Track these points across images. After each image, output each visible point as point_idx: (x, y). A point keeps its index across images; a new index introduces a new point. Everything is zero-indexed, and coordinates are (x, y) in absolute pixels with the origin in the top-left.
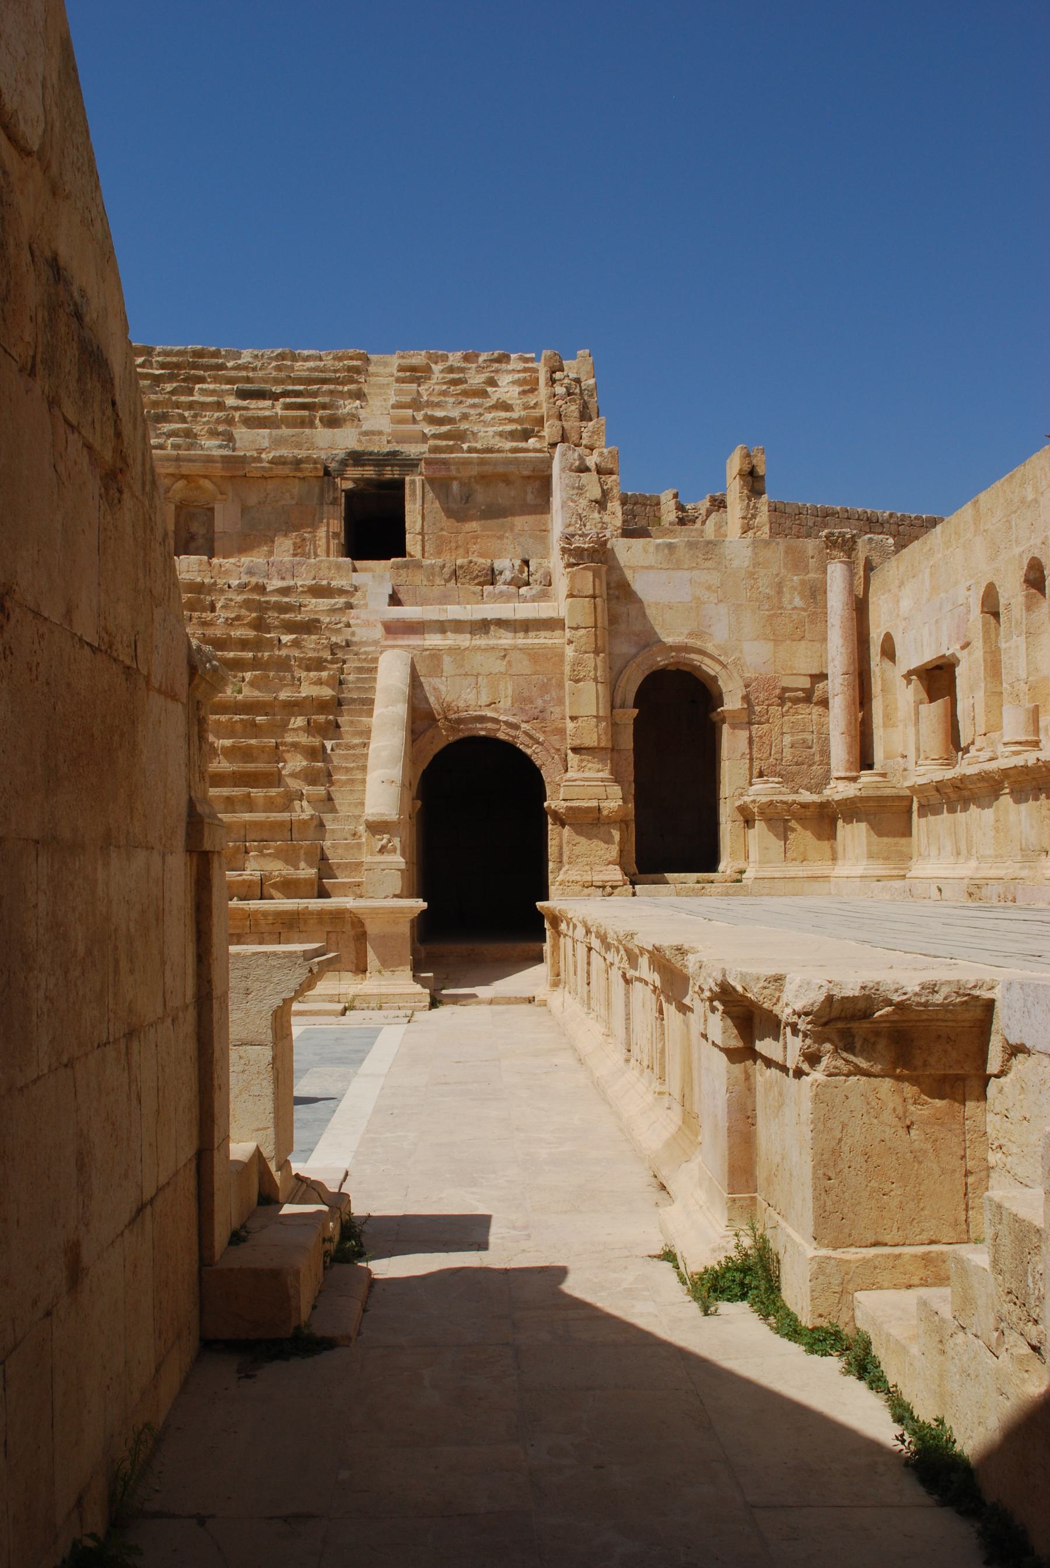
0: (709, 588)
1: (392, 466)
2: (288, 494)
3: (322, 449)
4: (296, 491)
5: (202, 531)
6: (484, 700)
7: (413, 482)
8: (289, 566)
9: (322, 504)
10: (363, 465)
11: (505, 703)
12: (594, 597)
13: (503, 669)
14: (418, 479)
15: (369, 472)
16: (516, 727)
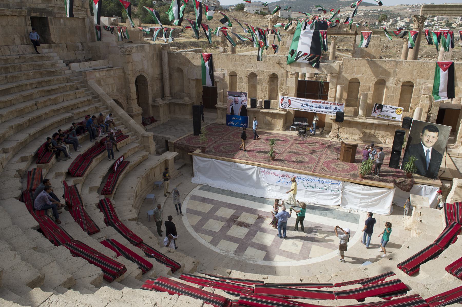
0: (144, 57)
4: (17, 21)
6: (111, 90)
7: (50, 19)
9: (26, 25)
10: (36, 12)
11: (115, 91)
12: (132, 63)
13: (113, 82)
14: (52, 17)
15: (38, 15)
16: (118, 96)
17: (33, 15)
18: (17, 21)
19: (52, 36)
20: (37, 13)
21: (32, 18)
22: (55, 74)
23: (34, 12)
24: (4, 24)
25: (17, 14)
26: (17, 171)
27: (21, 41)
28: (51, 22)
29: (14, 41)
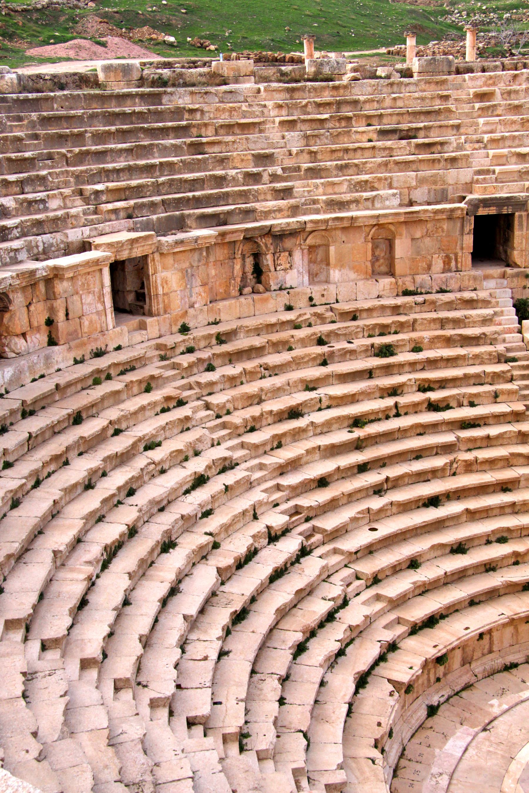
1: (508, 206)
2: (440, 229)
3: (450, 185)
5: (382, 254)
7: (521, 217)
8: (444, 280)
9: (463, 234)
10: (490, 206)
15: (492, 211)
17: (482, 212)
18: (445, 227)
19: (515, 253)
20: (492, 208)
21: (478, 219)
22: (482, 341)
23: (485, 206)
24: (418, 235)
25: (444, 217)
26: (268, 527)
27: (444, 266)
28: (521, 224)
29: (429, 267)
